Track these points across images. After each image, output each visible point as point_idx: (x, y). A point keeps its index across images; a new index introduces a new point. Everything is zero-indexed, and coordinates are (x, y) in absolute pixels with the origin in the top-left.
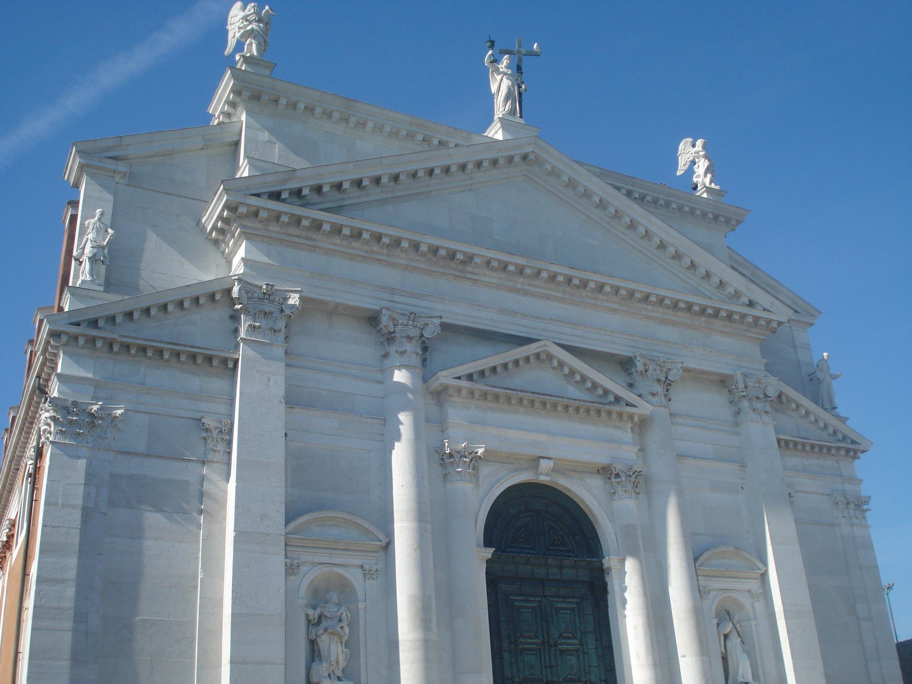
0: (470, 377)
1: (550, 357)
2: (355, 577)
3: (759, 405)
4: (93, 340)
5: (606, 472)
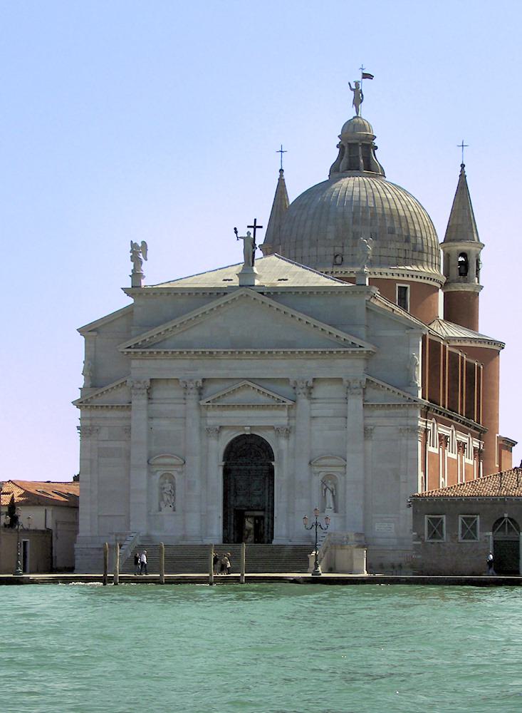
0: (214, 400)
1: (249, 386)
2: (175, 474)
3: (355, 391)
4: (86, 406)
5: (277, 430)
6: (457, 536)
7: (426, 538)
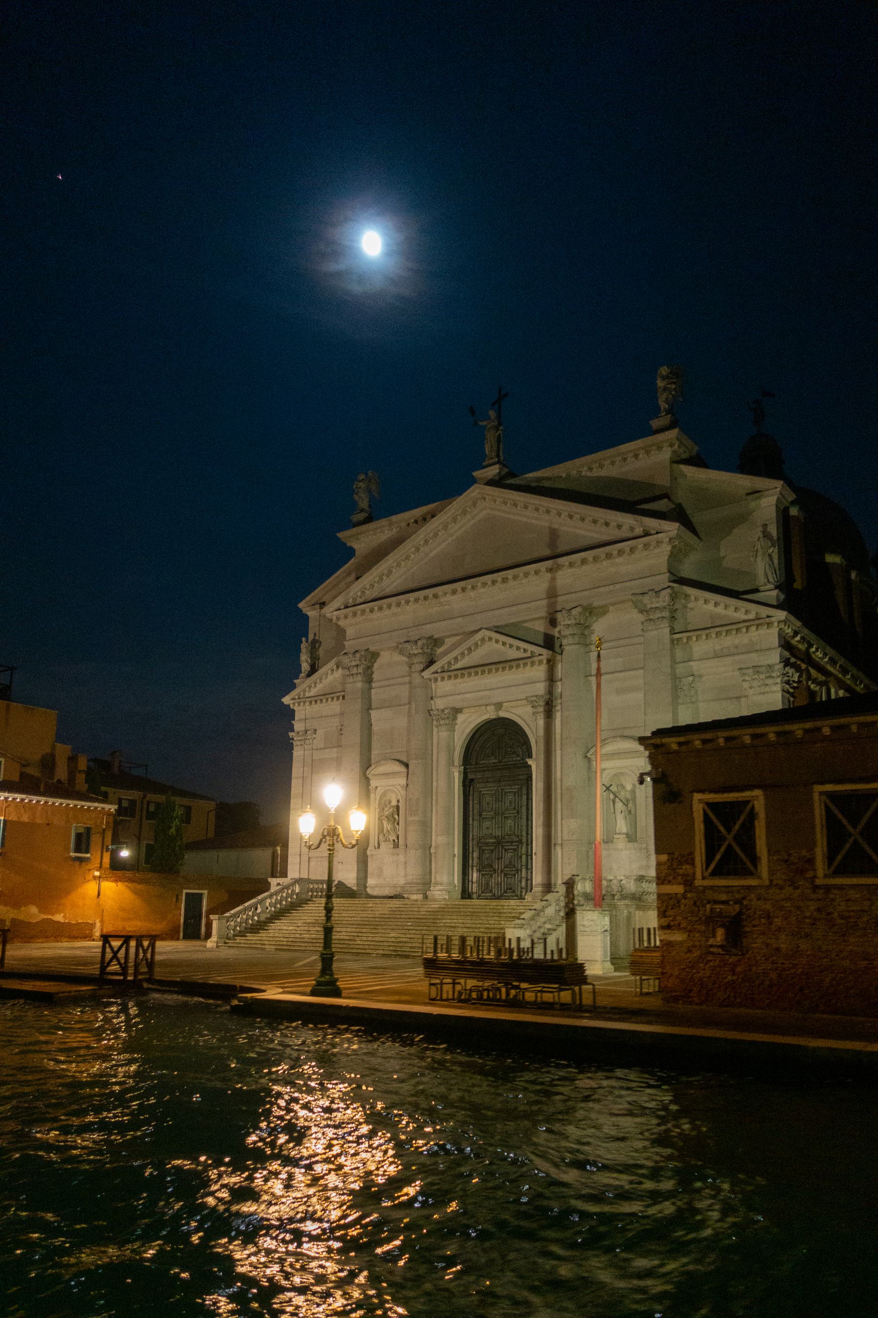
6: (811, 861)
7: (699, 875)
